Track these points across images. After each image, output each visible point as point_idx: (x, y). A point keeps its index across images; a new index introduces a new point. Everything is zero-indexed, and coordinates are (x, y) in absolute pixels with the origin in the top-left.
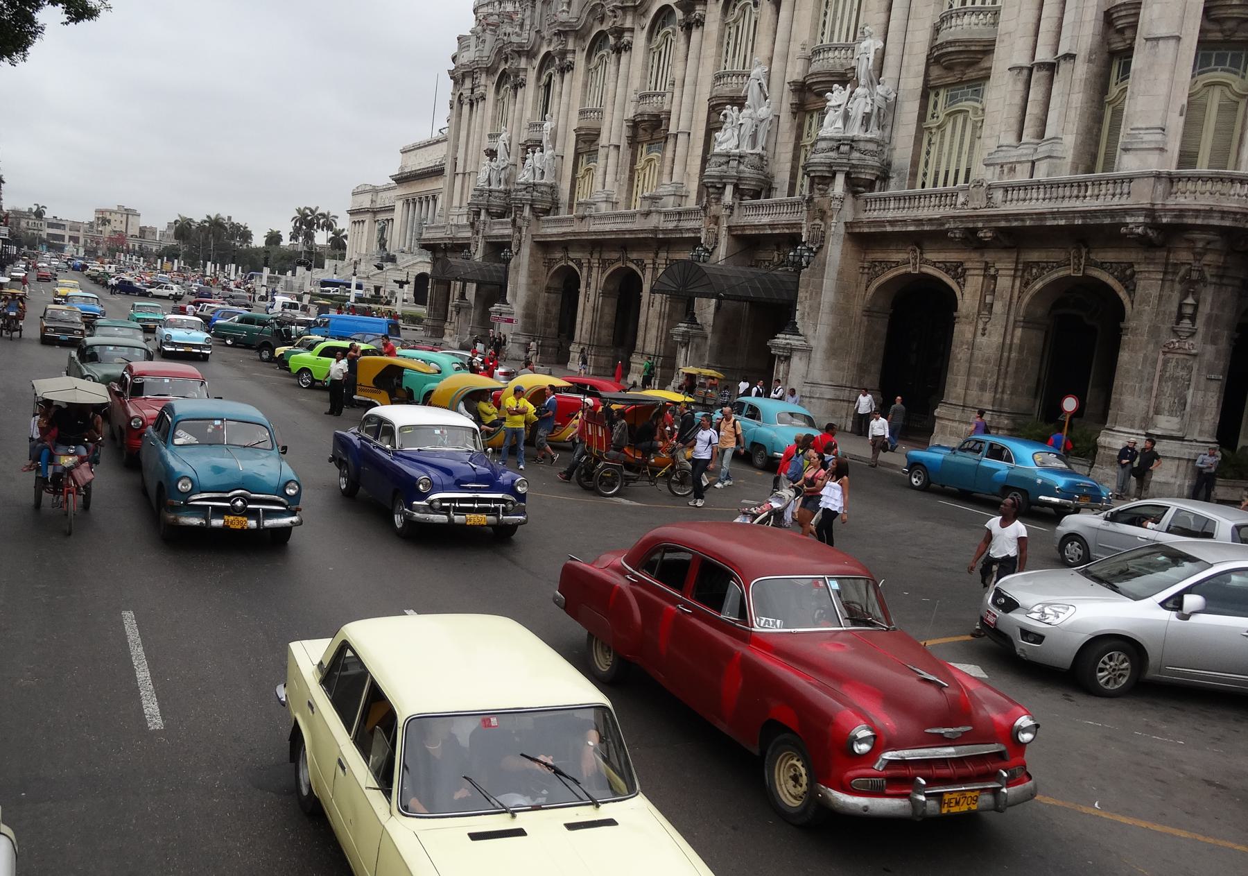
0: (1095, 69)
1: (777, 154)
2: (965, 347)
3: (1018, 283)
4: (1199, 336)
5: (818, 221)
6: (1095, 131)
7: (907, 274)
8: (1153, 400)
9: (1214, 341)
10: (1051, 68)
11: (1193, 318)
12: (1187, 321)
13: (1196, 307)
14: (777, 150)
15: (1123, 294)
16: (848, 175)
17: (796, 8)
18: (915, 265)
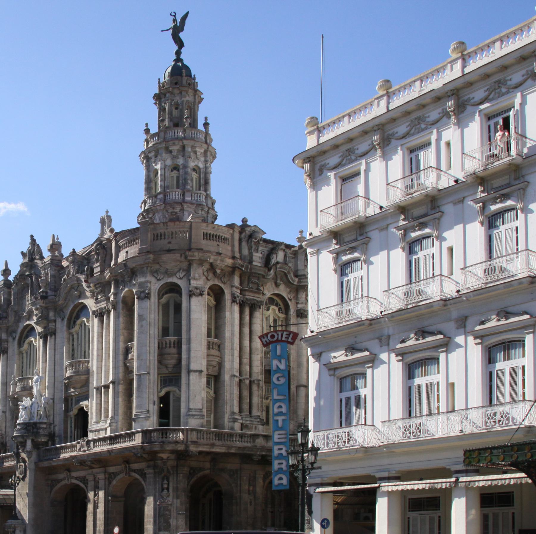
0: (124, 387)
1: (7, 433)
2: (91, 515)
3: (107, 483)
4: (171, 497)
5: (22, 464)
6: (128, 413)
7: (66, 485)
8: (157, 525)
9: (177, 498)
10: (107, 387)
11: (168, 489)
12: (166, 491)
13: (168, 485)
14: (7, 430)
15: (143, 483)
16: (33, 441)
17: (8, 359)
18: (68, 480)
